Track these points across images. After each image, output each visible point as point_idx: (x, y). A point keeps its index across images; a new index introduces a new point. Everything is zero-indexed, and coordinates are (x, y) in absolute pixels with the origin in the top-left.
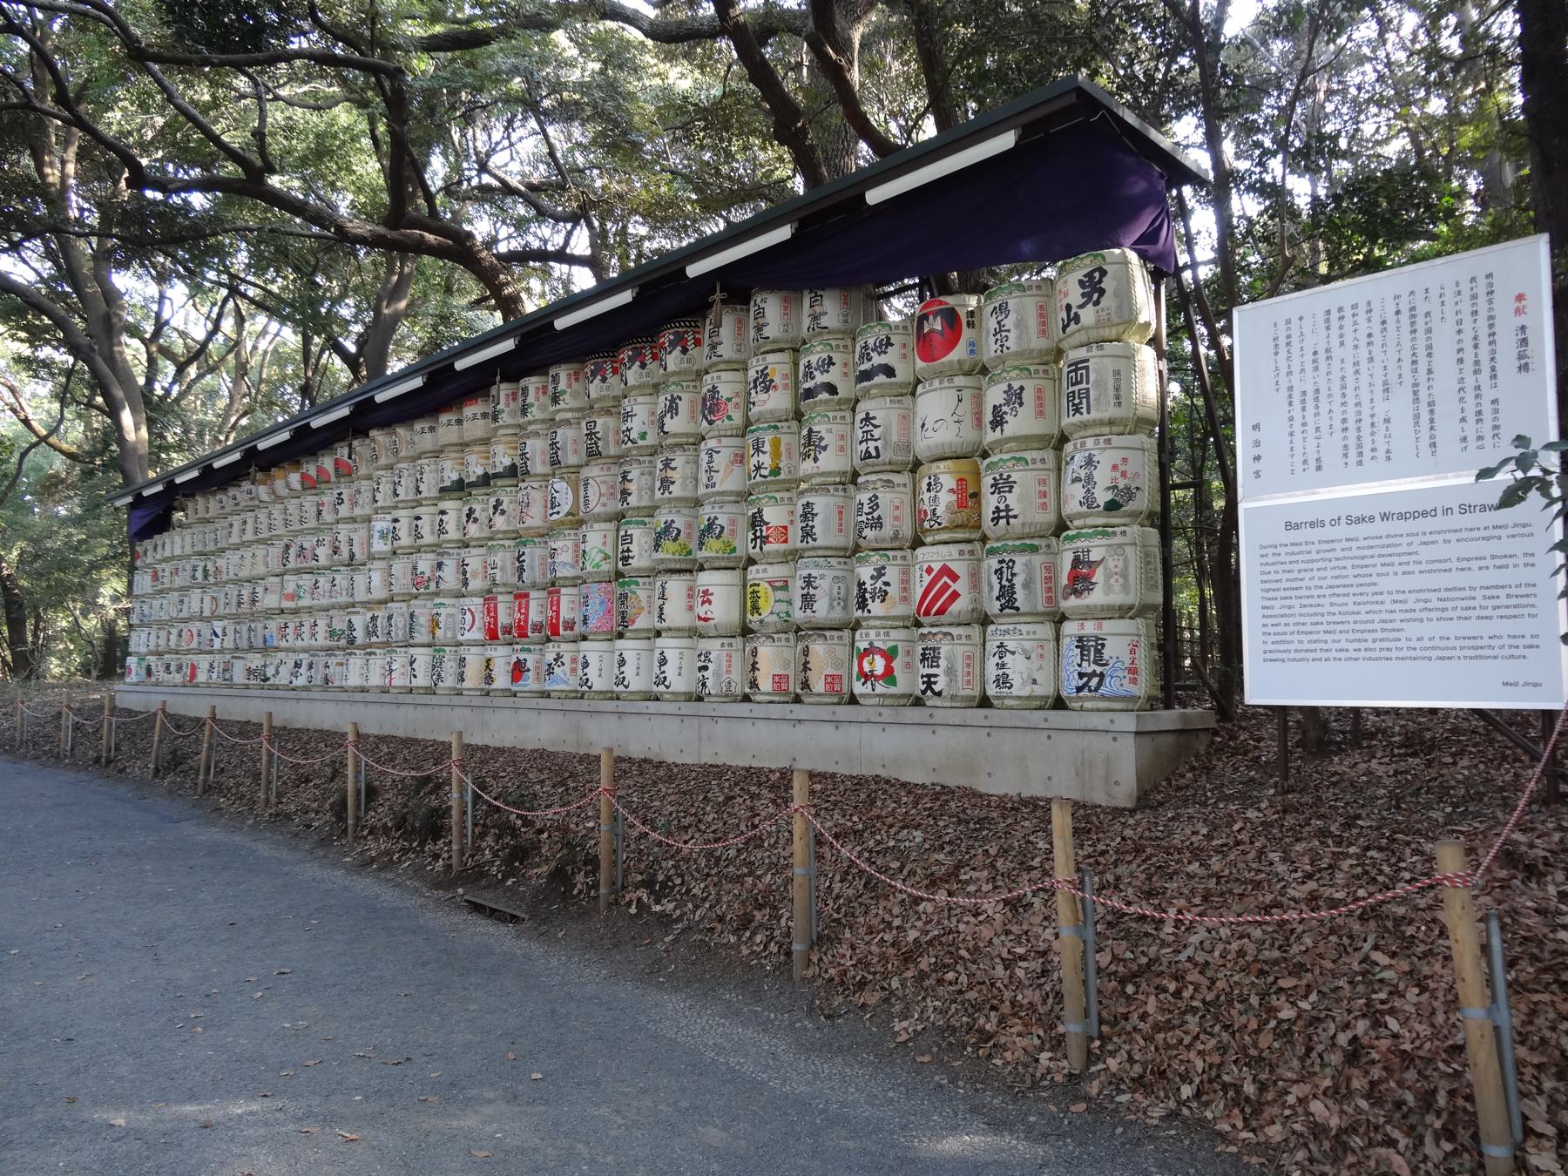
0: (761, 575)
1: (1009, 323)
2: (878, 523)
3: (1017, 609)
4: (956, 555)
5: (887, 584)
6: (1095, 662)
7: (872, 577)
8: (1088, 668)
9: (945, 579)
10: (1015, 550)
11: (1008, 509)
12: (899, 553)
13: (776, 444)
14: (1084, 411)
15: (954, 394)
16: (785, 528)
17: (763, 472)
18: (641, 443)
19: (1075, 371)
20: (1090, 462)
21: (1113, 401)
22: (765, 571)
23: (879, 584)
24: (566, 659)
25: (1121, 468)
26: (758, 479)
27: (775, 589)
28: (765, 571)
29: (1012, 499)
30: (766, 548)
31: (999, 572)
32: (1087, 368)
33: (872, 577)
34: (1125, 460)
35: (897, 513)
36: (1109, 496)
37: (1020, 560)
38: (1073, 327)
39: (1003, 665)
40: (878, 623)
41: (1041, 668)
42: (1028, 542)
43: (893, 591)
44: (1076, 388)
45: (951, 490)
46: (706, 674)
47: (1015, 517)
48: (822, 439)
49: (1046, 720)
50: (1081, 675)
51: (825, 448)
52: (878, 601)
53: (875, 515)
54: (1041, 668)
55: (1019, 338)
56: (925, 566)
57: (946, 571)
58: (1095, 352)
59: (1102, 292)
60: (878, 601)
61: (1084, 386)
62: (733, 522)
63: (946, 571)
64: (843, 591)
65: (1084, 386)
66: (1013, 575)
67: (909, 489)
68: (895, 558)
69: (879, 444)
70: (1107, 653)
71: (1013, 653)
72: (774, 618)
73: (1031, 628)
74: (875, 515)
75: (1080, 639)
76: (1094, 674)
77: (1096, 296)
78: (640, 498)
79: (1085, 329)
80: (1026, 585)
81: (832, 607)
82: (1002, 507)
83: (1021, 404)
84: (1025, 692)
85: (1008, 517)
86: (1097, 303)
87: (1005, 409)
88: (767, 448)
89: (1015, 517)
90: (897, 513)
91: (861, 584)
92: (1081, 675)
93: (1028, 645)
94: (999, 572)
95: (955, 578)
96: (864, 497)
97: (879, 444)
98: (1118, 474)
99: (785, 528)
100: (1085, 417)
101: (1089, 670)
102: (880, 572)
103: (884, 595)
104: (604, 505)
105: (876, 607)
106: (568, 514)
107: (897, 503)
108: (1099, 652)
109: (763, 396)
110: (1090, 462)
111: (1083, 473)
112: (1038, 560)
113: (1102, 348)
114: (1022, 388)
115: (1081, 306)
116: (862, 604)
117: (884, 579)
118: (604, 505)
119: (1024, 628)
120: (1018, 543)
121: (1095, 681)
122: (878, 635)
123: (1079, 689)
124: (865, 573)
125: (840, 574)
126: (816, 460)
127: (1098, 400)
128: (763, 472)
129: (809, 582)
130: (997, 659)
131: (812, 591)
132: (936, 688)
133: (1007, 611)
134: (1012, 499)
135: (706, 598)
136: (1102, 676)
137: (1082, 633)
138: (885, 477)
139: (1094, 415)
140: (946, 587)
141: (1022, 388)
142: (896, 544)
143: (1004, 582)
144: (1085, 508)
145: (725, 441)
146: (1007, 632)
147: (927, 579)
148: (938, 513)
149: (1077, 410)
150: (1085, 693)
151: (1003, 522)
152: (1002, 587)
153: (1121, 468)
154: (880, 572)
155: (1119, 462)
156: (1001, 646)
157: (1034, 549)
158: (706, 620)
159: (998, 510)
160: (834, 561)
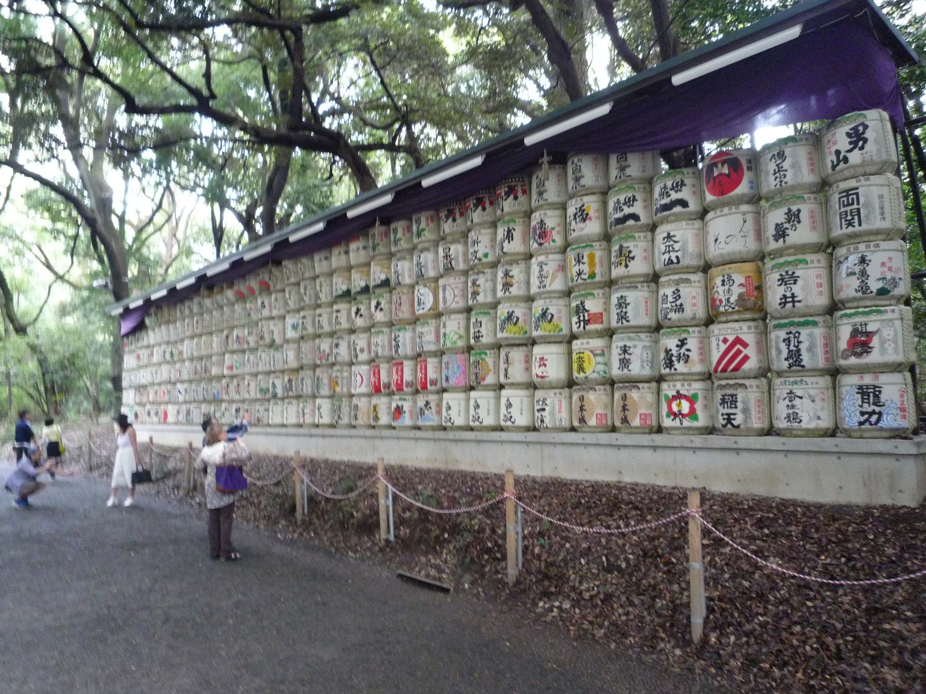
0: (585, 346)
1: (786, 165)
2: (681, 308)
3: (803, 366)
4: (745, 329)
5: (688, 350)
6: (875, 404)
7: (677, 346)
8: (868, 408)
9: (738, 346)
10: (800, 324)
11: (793, 296)
12: (697, 329)
13: (592, 257)
14: (856, 224)
15: (740, 217)
16: (601, 314)
17: (583, 276)
18: (484, 260)
19: (848, 196)
20: (863, 260)
21: (879, 217)
22: (588, 343)
23: (683, 351)
24: (433, 405)
25: (888, 264)
26: (579, 280)
27: (595, 355)
28: (588, 343)
29: (797, 289)
30: (589, 327)
31: (787, 341)
32: (857, 194)
33: (677, 346)
34: (890, 259)
35: (694, 301)
36: (880, 285)
37: (804, 332)
39: (793, 407)
40: (681, 377)
41: (822, 409)
43: (694, 355)
44: (848, 208)
45: (741, 285)
46: (544, 413)
47: (799, 301)
48: (630, 252)
49: (896, 447)
50: (862, 414)
51: (633, 258)
52: (682, 362)
54: (822, 409)
55: (795, 174)
56: (721, 338)
57: (738, 341)
58: (863, 182)
59: (865, 141)
60: (682, 362)
61: (855, 206)
62: (559, 311)
63: (738, 341)
64: (650, 356)
65: (855, 206)
66: (799, 342)
67: (702, 284)
68: (694, 332)
70: (883, 398)
71: (801, 398)
72: (596, 375)
73: (814, 379)
75: (861, 387)
76: (874, 412)
77: (860, 143)
78: (486, 296)
79: (853, 167)
80: (810, 349)
81: (643, 367)
82: (789, 294)
83: (799, 222)
84: (812, 425)
85: (793, 302)
86: (862, 148)
87: (786, 225)
88: (586, 259)
89: (799, 301)
90: (694, 301)
91: (667, 351)
92: (862, 414)
93: (812, 392)
94: (787, 341)
95: (745, 345)
96: (669, 291)
97: (679, 254)
98: (886, 269)
99: (601, 314)
100: (857, 228)
101: (870, 410)
102: (683, 343)
103: (687, 359)
104: (457, 302)
105: (680, 367)
106: (430, 309)
107: (694, 294)
108: (877, 397)
109: (581, 225)
110: (863, 260)
111: (857, 269)
113: (868, 179)
114: (799, 211)
115: (850, 151)
116: (670, 364)
117: (686, 347)
118: (457, 302)
121: (874, 418)
122: (683, 385)
123: (861, 423)
124: (671, 343)
125: (648, 344)
126: (626, 266)
127: (867, 216)
128: (583, 276)
129: (625, 350)
130: (787, 402)
131: (627, 356)
132: (735, 423)
133: (795, 368)
134: (797, 289)
135: (543, 362)
136: (880, 414)
137: (861, 383)
139: (865, 227)
140: (739, 352)
141: (799, 211)
142: (694, 323)
143: (792, 348)
144: (860, 294)
145: (551, 257)
146: (796, 383)
147: (723, 347)
148: (732, 300)
149: (850, 224)
150: (867, 426)
151: (789, 305)
152: (790, 351)
153: (888, 264)
154: (683, 343)
155: (886, 260)
156: (791, 392)
157: (815, 324)
158: (542, 377)
159: (785, 297)
160: (643, 336)
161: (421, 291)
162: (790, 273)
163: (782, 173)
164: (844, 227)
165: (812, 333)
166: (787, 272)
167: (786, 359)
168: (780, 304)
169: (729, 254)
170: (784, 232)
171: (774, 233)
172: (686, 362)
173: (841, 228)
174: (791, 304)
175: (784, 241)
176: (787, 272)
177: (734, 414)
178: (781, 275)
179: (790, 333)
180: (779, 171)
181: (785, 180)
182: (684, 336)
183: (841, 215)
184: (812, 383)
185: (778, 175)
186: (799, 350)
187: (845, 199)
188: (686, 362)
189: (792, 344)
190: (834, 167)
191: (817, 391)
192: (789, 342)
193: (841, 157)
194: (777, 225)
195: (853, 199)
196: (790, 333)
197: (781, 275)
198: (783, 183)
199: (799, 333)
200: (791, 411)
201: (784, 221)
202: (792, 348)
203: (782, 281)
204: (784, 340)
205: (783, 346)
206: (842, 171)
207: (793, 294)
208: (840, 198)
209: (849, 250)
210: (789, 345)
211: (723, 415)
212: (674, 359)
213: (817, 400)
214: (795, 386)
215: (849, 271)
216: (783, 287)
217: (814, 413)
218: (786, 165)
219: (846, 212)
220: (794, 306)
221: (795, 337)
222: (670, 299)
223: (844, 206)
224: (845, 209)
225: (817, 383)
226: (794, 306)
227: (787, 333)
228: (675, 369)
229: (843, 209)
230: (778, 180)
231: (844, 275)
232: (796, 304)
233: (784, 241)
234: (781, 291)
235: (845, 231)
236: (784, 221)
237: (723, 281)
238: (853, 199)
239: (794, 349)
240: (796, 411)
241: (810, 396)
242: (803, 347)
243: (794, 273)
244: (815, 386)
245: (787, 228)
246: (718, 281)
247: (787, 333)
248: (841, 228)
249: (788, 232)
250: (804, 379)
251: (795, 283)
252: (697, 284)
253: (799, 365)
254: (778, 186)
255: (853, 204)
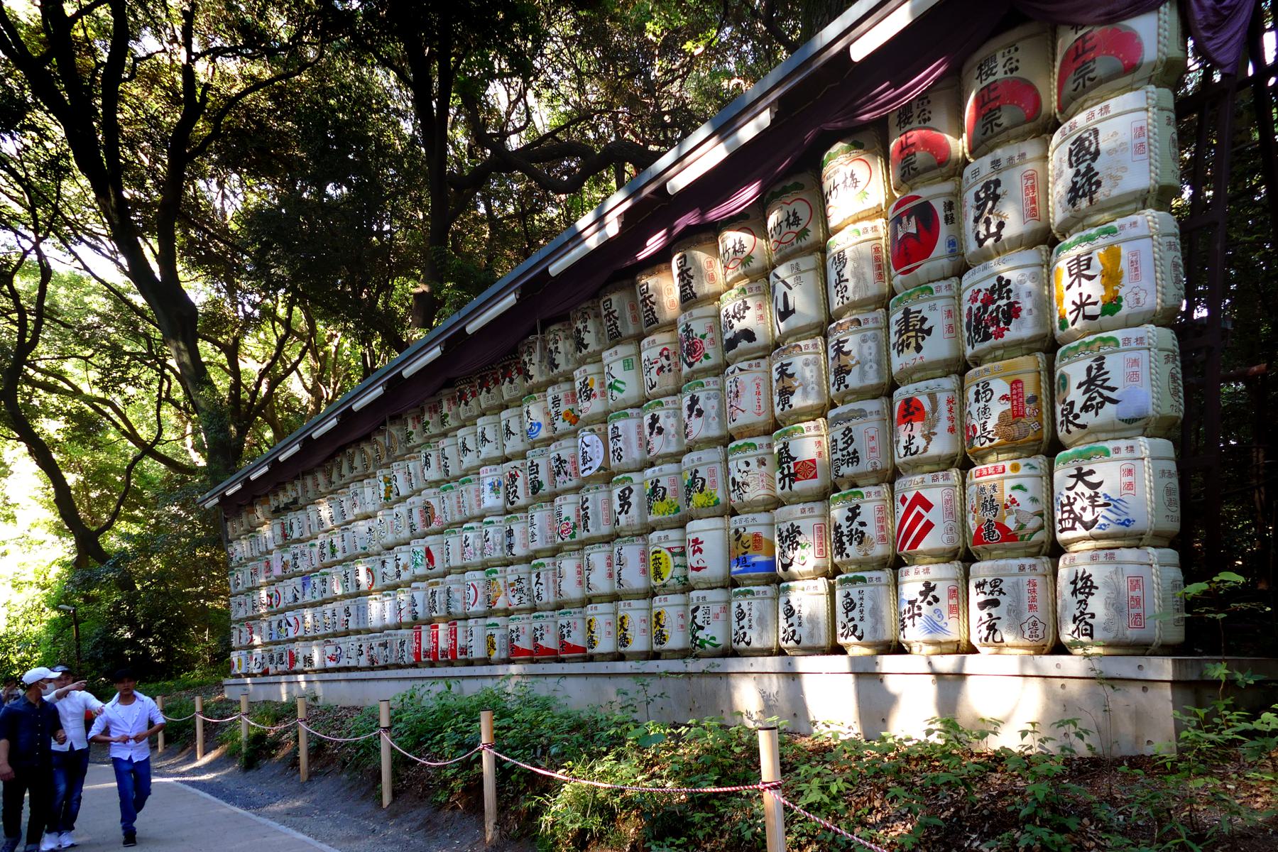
2: (854, 458)
5: (862, 524)
23: (855, 525)
33: (848, 519)
52: (855, 543)
53: (851, 449)
60: (855, 543)
74: (851, 449)
102: (854, 513)
117: (859, 519)
154: (854, 513)
161: (587, 440)
172: (860, 543)
182: (855, 501)
188: (860, 543)
212: (845, 539)
222: (841, 445)
228: (848, 555)
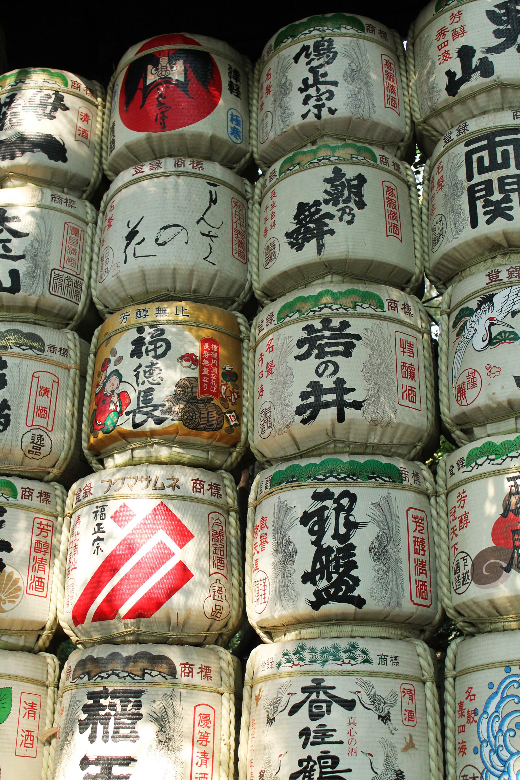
1: (334, 71)
3: (360, 602)
10: (355, 473)
12: (37, 487)
15: (202, 189)
35: (43, 402)
38: (477, 80)
39: (323, 735)
41: (410, 745)
42: (384, 460)
44: (494, 176)
47: (357, 405)
66: (352, 526)
67: (74, 356)
68: (28, 493)
69: (21, 266)
71: (349, 705)
73: (388, 648)
79: (503, 86)
80: (381, 550)
82: (328, 382)
83: (361, 205)
85: (341, 406)
87: (325, 208)
89: (357, 405)
90: (43, 402)
93: (384, 688)
97: (21, 266)
107: (46, 381)
112: (403, 499)
114: (361, 179)
119: (375, 648)
120: (361, 459)
133: (332, 608)
134: (351, 370)
138: (26, 329)
141: (361, 179)
143: (328, 541)
151: (327, 415)
152: (321, 552)
156: (317, 686)
157: (395, 477)
162: (335, 323)
163: (323, 88)
164: (482, 218)
165: (387, 500)
166: (326, 321)
167: (307, 578)
168: (300, 411)
169: (161, 273)
170: (320, 223)
171: (292, 226)
173: (474, 224)
174: (333, 411)
175: (320, 248)
176: (326, 321)
177: (128, 761)
178: (309, 329)
179: (327, 495)
180: (316, 82)
181: (329, 104)
183: (471, 191)
184: (383, 659)
185: (312, 91)
186: (349, 550)
187: (485, 154)
189: (330, 532)
190: (453, 87)
191: (395, 685)
192: (322, 522)
193: (475, 62)
194: (302, 207)
195: (505, 153)
196: (327, 495)
197: (309, 329)
198: (325, 112)
199: (353, 498)
200: (315, 752)
201: (321, 197)
202: (328, 541)
203: (310, 344)
204: (305, 519)
205: (301, 538)
206: (473, 96)
207: (340, 382)
208: (468, 156)
209: (493, 277)
210: (321, 534)
211: (85, 762)
213: (395, 714)
214: (332, 666)
215: (495, 331)
216: (313, 362)
217: (388, 761)
218: (334, 71)
219: (489, 183)
220: (341, 417)
221: (339, 509)
223: (482, 170)
224: (485, 177)
225: (395, 659)
226: (341, 417)
227: (316, 497)
229: (477, 178)
230: (312, 102)
231: (479, 343)
232: (349, 412)
233: (320, 248)
234: (305, 372)
235: (484, 229)
236: (321, 197)
237: (138, 343)
238: (505, 153)
239: (335, 544)
240: (334, 750)
241: (374, 699)
242: (362, 540)
243: (345, 325)
244: (389, 668)
245: (330, 216)
246: (123, 345)
247: (316, 497)
248: (474, 224)
249: (332, 224)
250: (361, 644)
251: (347, 354)
252: (56, 357)
253: (346, 599)
254: (311, 118)
255: (506, 164)
